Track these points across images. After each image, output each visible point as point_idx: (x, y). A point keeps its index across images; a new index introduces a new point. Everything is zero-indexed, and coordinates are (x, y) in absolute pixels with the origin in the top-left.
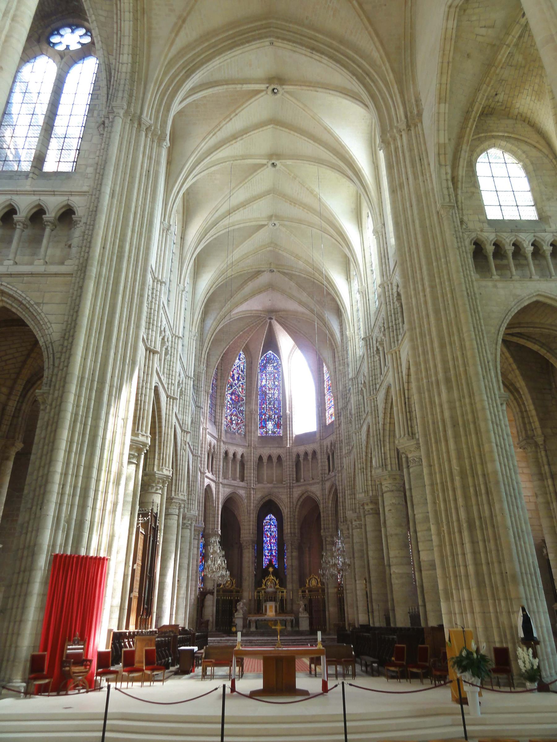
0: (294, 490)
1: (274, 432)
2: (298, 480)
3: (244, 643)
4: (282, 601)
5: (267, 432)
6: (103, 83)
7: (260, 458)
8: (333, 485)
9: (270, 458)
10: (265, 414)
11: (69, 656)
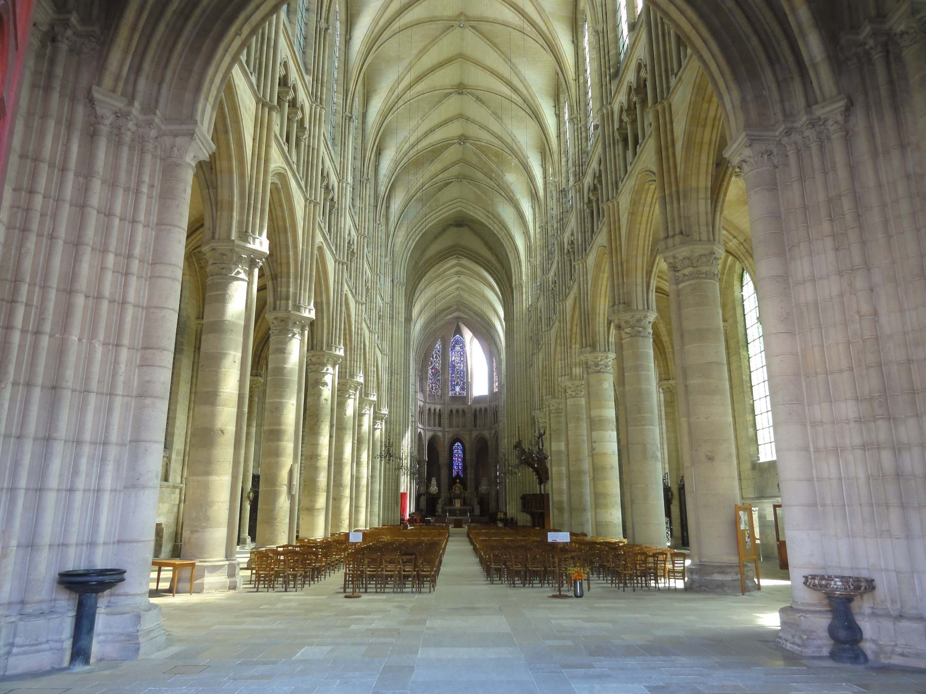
0: (473, 432)
1: (460, 394)
2: (475, 426)
3: (449, 516)
4: (464, 498)
5: (455, 394)
7: (451, 411)
8: (496, 432)
9: (457, 411)
10: (454, 381)
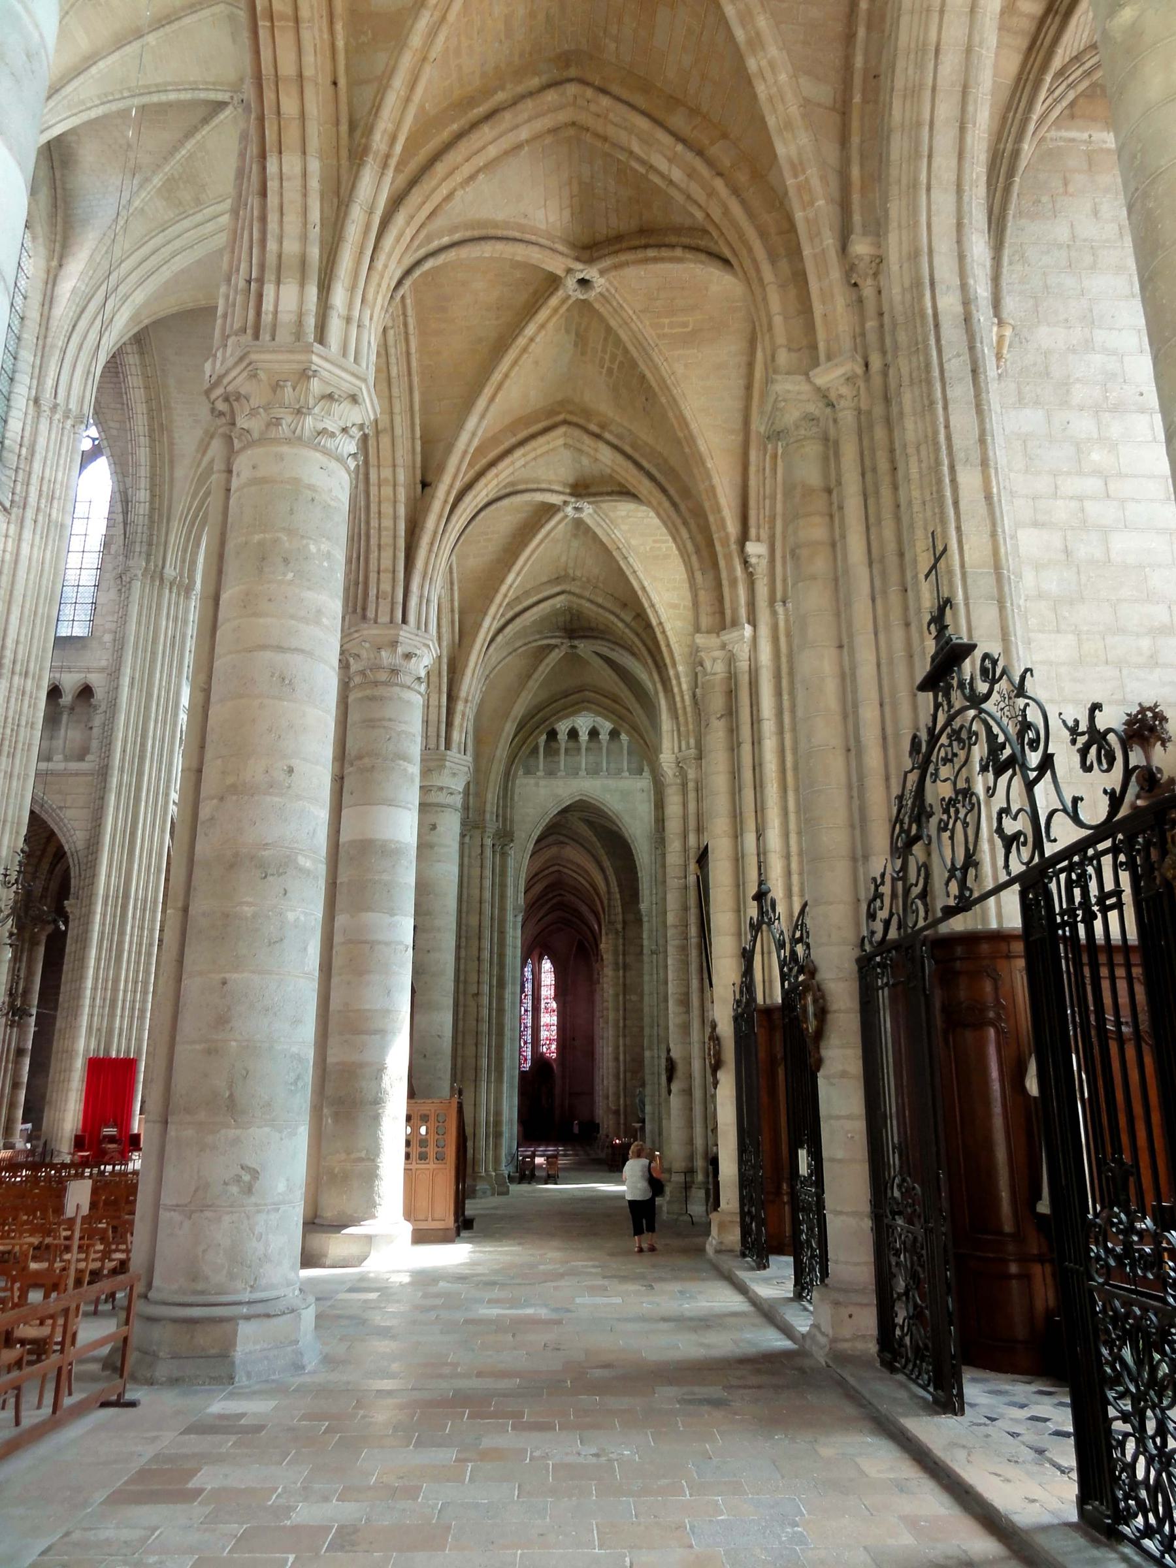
6: (120, 518)
11: (105, 1137)
